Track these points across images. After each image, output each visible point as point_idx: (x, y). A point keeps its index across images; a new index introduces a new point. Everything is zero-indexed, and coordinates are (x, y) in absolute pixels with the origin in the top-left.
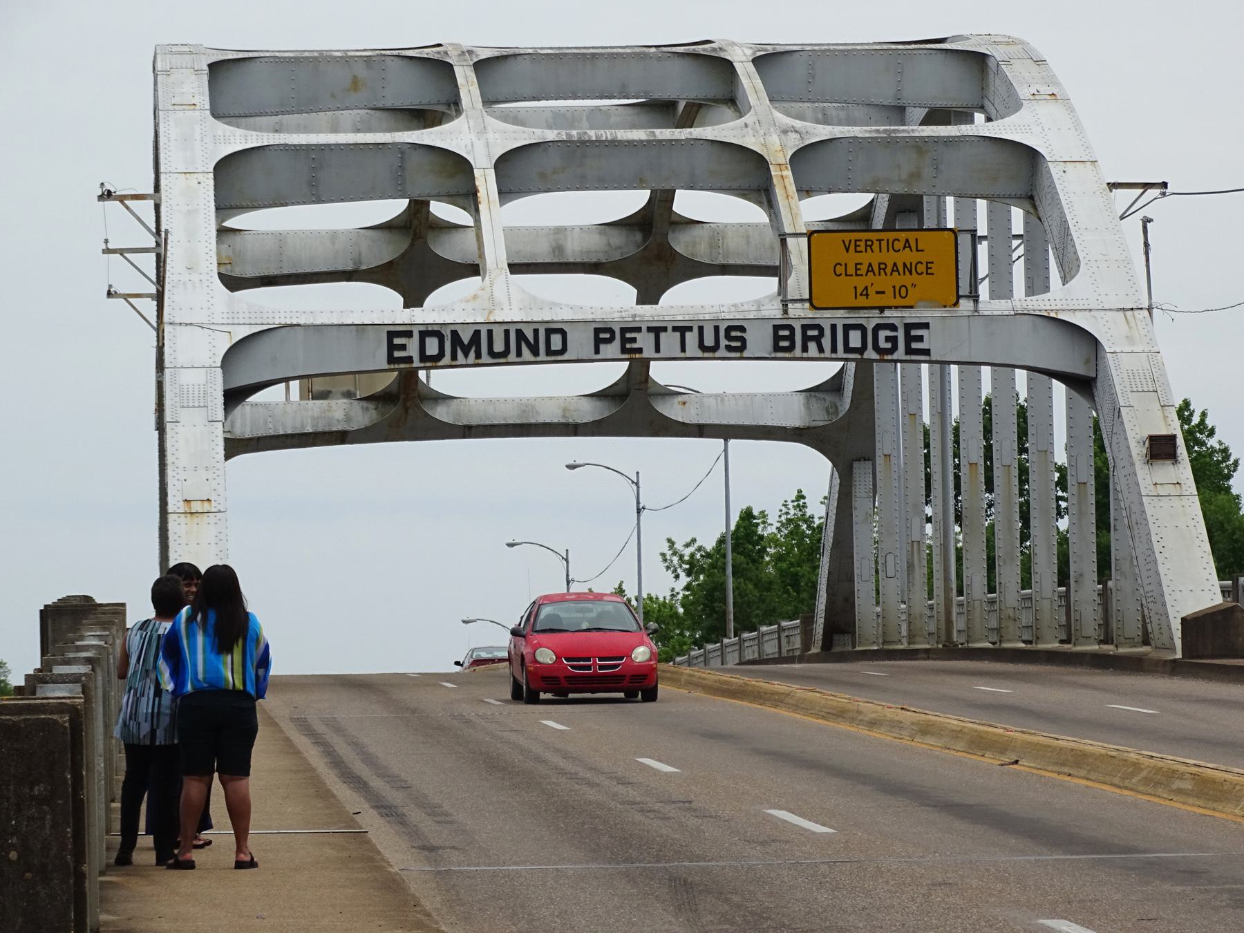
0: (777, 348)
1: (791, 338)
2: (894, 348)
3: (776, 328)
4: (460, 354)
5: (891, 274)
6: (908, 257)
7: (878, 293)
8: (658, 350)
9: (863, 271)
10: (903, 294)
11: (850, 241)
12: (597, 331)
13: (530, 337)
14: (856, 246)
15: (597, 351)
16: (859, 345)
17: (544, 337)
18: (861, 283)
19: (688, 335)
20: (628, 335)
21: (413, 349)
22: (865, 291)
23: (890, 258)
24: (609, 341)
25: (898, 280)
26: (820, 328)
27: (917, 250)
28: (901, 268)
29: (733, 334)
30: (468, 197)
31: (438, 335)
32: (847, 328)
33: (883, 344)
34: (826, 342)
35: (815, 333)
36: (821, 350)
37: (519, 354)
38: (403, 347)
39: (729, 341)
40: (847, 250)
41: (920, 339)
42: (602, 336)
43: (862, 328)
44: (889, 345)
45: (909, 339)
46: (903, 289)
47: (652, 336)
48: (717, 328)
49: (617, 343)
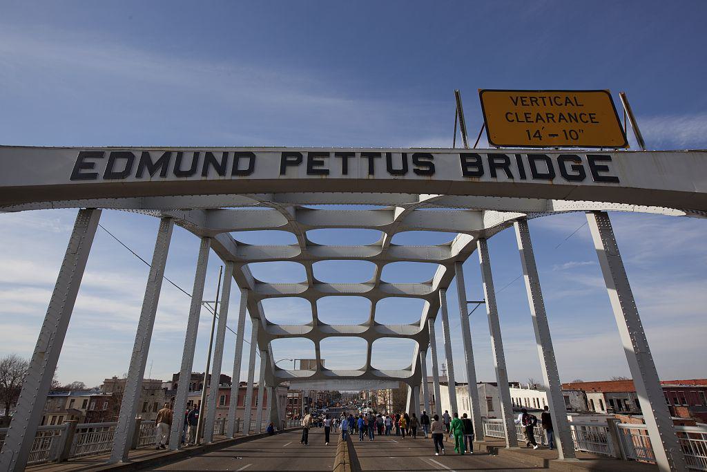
0: (466, 174)
1: (479, 164)
4: (146, 172)
5: (559, 121)
7: (550, 135)
9: (533, 118)
11: (517, 98)
12: (285, 155)
13: (219, 158)
14: (522, 101)
15: (283, 172)
17: (228, 160)
18: (533, 128)
23: (556, 111)
25: (568, 126)
27: (577, 105)
28: (567, 117)
29: (420, 160)
31: (127, 154)
32: (532, 158)
33: (570, 172)
34: (514, 168)
36: (510, 175)
38: (91, 166)
39: (417, 165)
40: (516, 104)
42: (289, 159)
43: (543, 157)
44: (577, 173)
47: (340, 161)
48: (404, 156)
49: (304, 166)
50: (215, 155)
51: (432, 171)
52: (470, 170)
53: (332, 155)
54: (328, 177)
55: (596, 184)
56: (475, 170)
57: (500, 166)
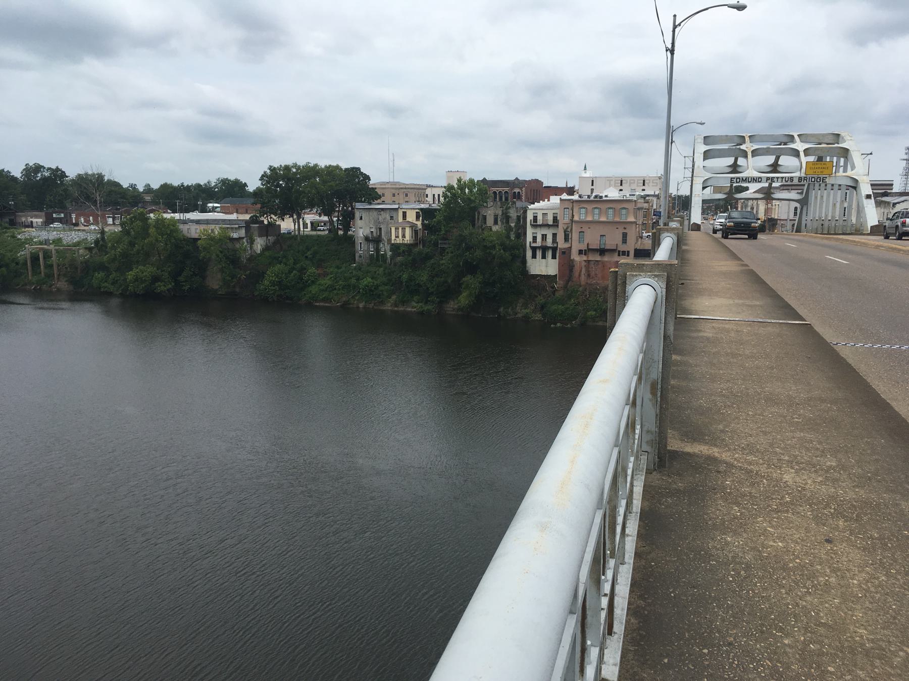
3: (799, 178)
6: (824, 166)
12: (767, 178)
21: (735, 180)
23: (820, 166)
25: (822, 170)
26: (806, 177)
30: (746, 156)
31: (739, 178)
33: (818, 181)
36: (807, 181)
41: (825, 180)
45: (823, 180)
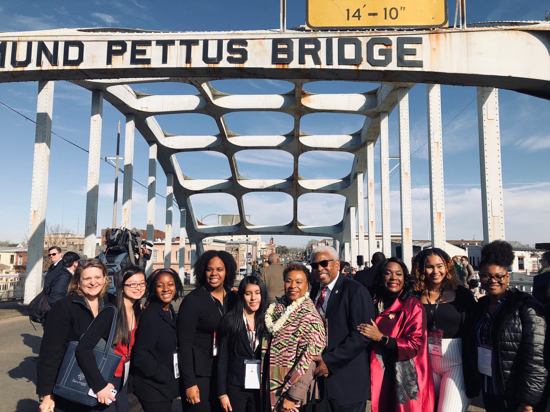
0: (275, 60)
1: (289, 51)
2: (388, 60)
3: (276, 42)
7: (370, 14)
8: (165, 60)
10: (394, 15)
15: (109, 62)
16: (353, 57)
19: (193, 48)
20: (138, 48)
22: (357, 13)
24: (121, 53)
26: (316, 41)
29: (234, 47)
33: (377, 56)
34: (322, 54)
35: (312, 46)
36: (317, 61)
37: (39, 63)
41: (413, 52)
42: (114, 48)
44: (383, 58)
45: (402, 52)
46: (394, 11)
49: (128, 55)
50: (45, 43)
51: (244, 58)
52: (280, 56)
53: (154, 43)
54: (149, 66)
55: (400, 69)
56: (285, 56)
57: (309, 52)
